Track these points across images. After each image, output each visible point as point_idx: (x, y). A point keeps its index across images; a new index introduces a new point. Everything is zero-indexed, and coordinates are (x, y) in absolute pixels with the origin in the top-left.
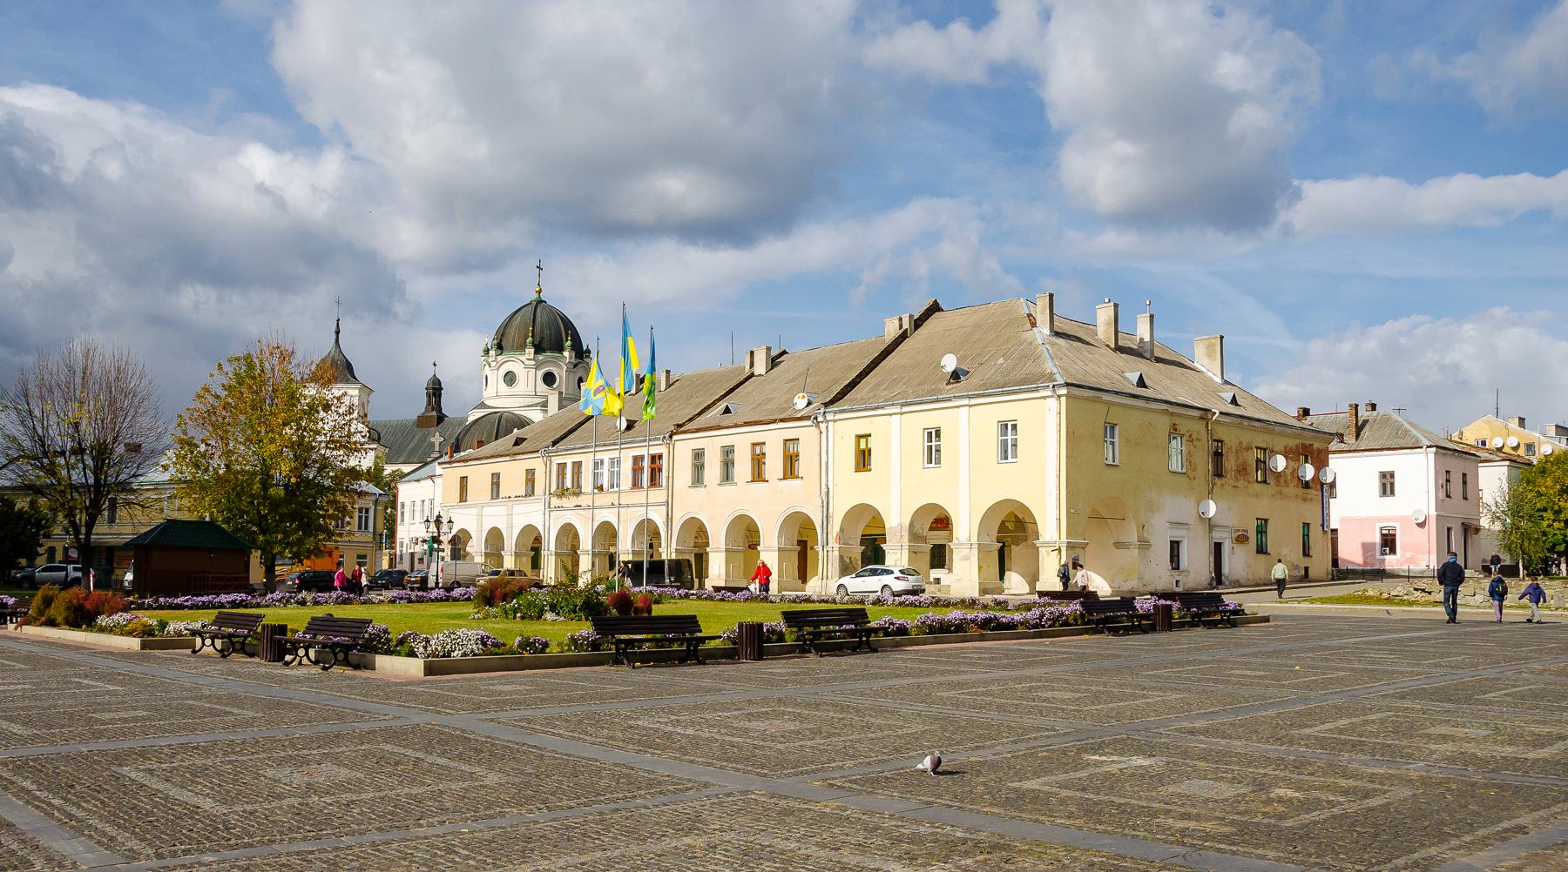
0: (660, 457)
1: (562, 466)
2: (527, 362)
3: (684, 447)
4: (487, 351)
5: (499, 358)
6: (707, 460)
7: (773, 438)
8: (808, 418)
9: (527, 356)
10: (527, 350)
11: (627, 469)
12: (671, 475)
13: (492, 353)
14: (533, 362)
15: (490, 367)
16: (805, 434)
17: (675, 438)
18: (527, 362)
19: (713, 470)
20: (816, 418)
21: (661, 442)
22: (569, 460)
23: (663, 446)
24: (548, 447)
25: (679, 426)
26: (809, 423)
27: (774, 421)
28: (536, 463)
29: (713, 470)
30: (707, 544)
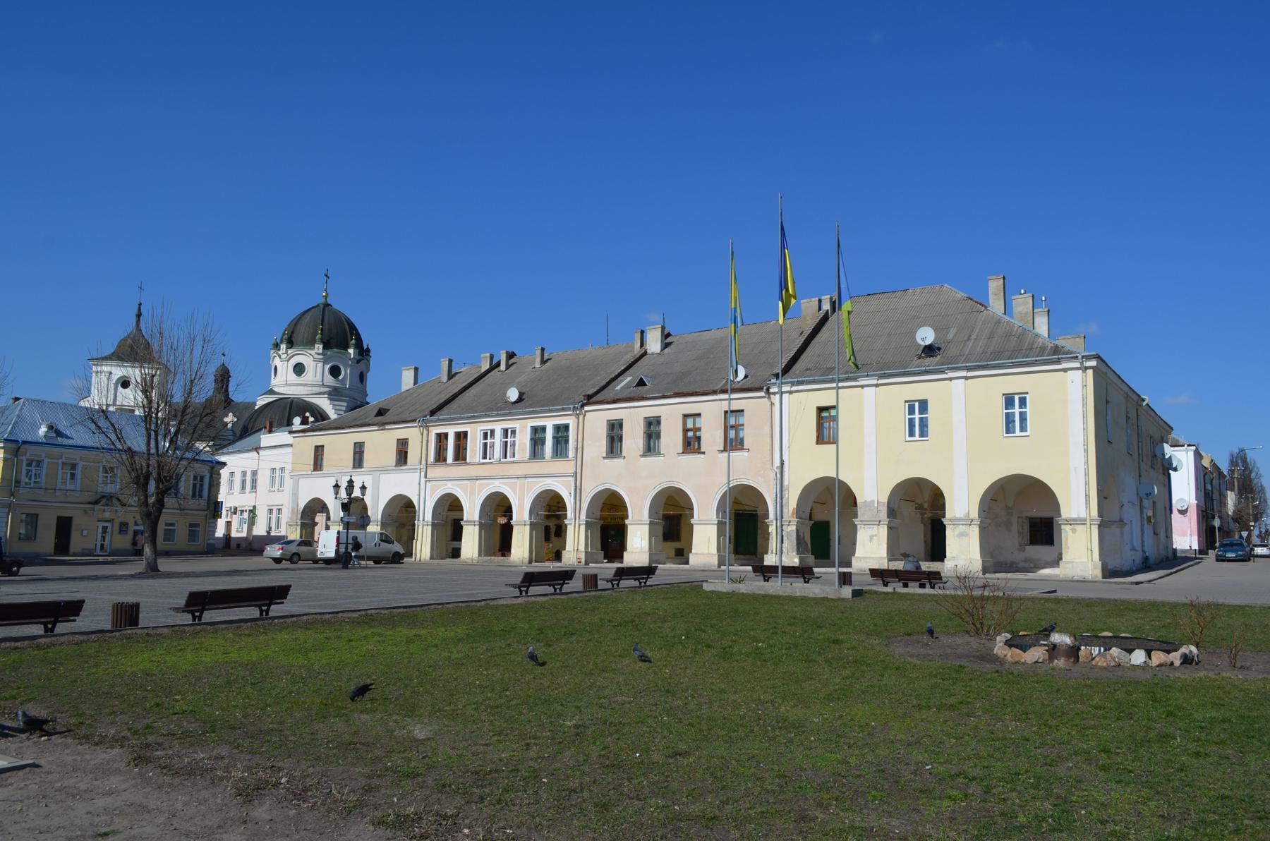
0: (566, 427)
1: (442, 438)
2: (316, 356)
3: (597, 418)
4: (277, 346)
5: (290, 351)
6: (626, 432)
7: (711, 410)
8: (760, 389)
9: (316, 351)
10: (316, 346)
11: (523, 440)
12: (580, 445)
13: (283, 346)
14: (321, 357)
15: (280, 358)
16: (751, 404)
17: (586, 408)
18: (316, 356)
19: (633, 439)
20: (768, 390)
21: (571, 413)
22: (451, 431)
23: (574, 417)
24: (426, 416)
25: (589, 397)
26: (762, 394)
27: (715, 392)
28: (411, 433)
29: (633, 439)
30: (627, 517)
